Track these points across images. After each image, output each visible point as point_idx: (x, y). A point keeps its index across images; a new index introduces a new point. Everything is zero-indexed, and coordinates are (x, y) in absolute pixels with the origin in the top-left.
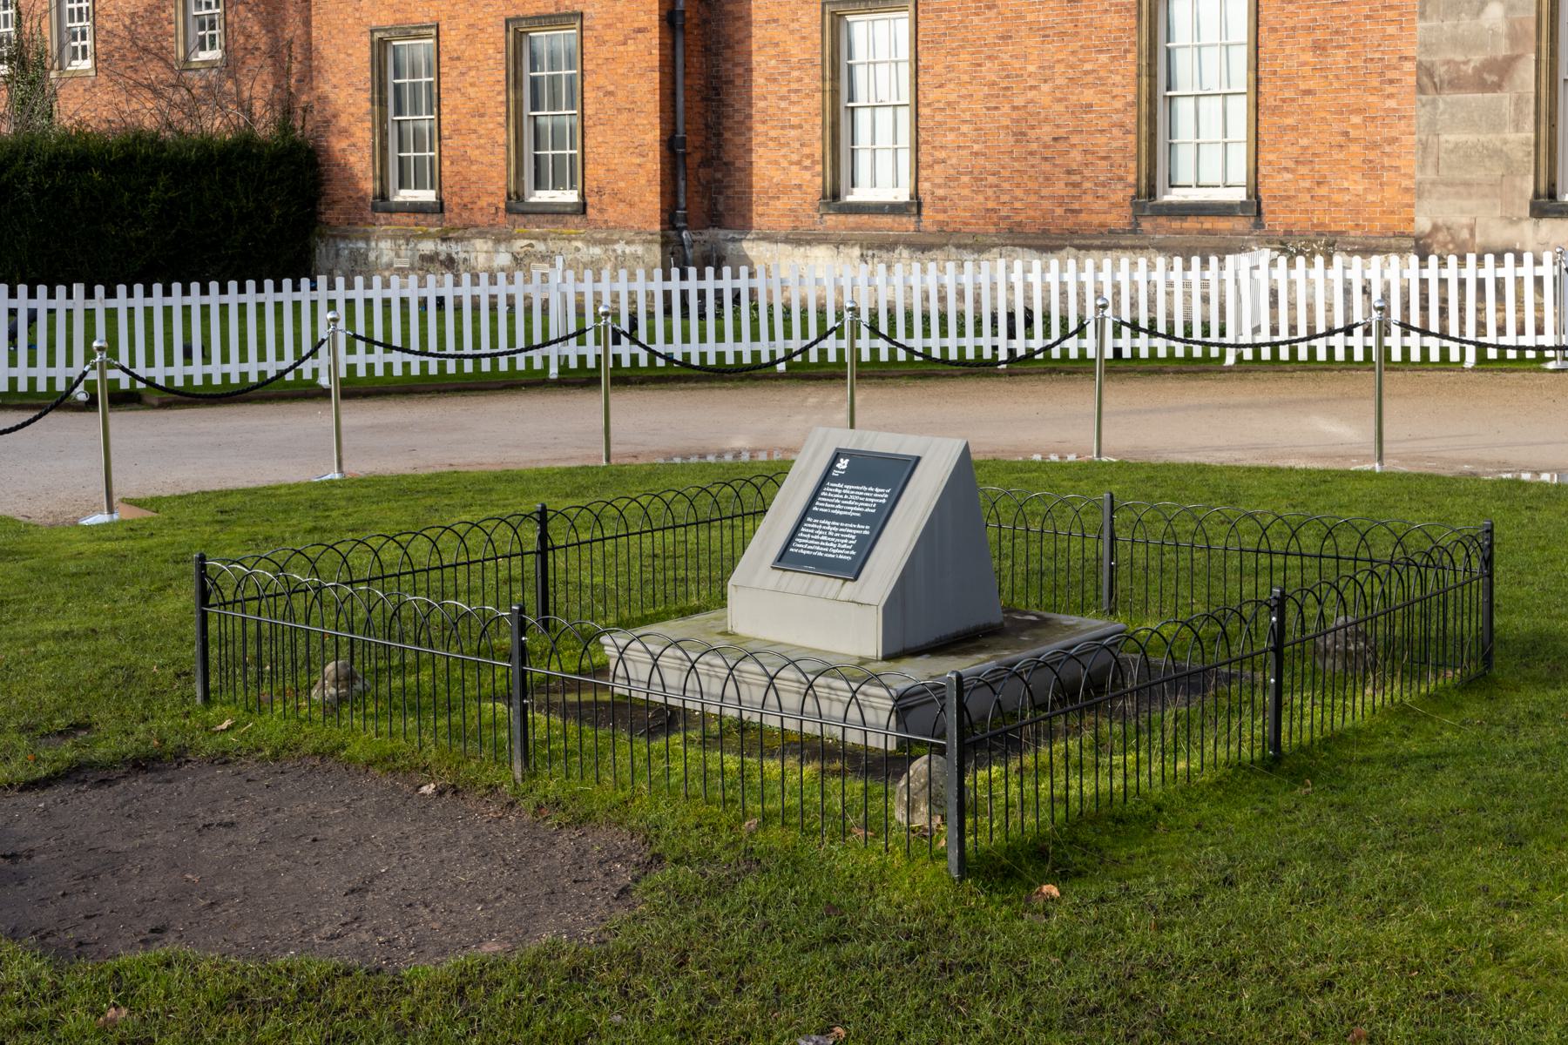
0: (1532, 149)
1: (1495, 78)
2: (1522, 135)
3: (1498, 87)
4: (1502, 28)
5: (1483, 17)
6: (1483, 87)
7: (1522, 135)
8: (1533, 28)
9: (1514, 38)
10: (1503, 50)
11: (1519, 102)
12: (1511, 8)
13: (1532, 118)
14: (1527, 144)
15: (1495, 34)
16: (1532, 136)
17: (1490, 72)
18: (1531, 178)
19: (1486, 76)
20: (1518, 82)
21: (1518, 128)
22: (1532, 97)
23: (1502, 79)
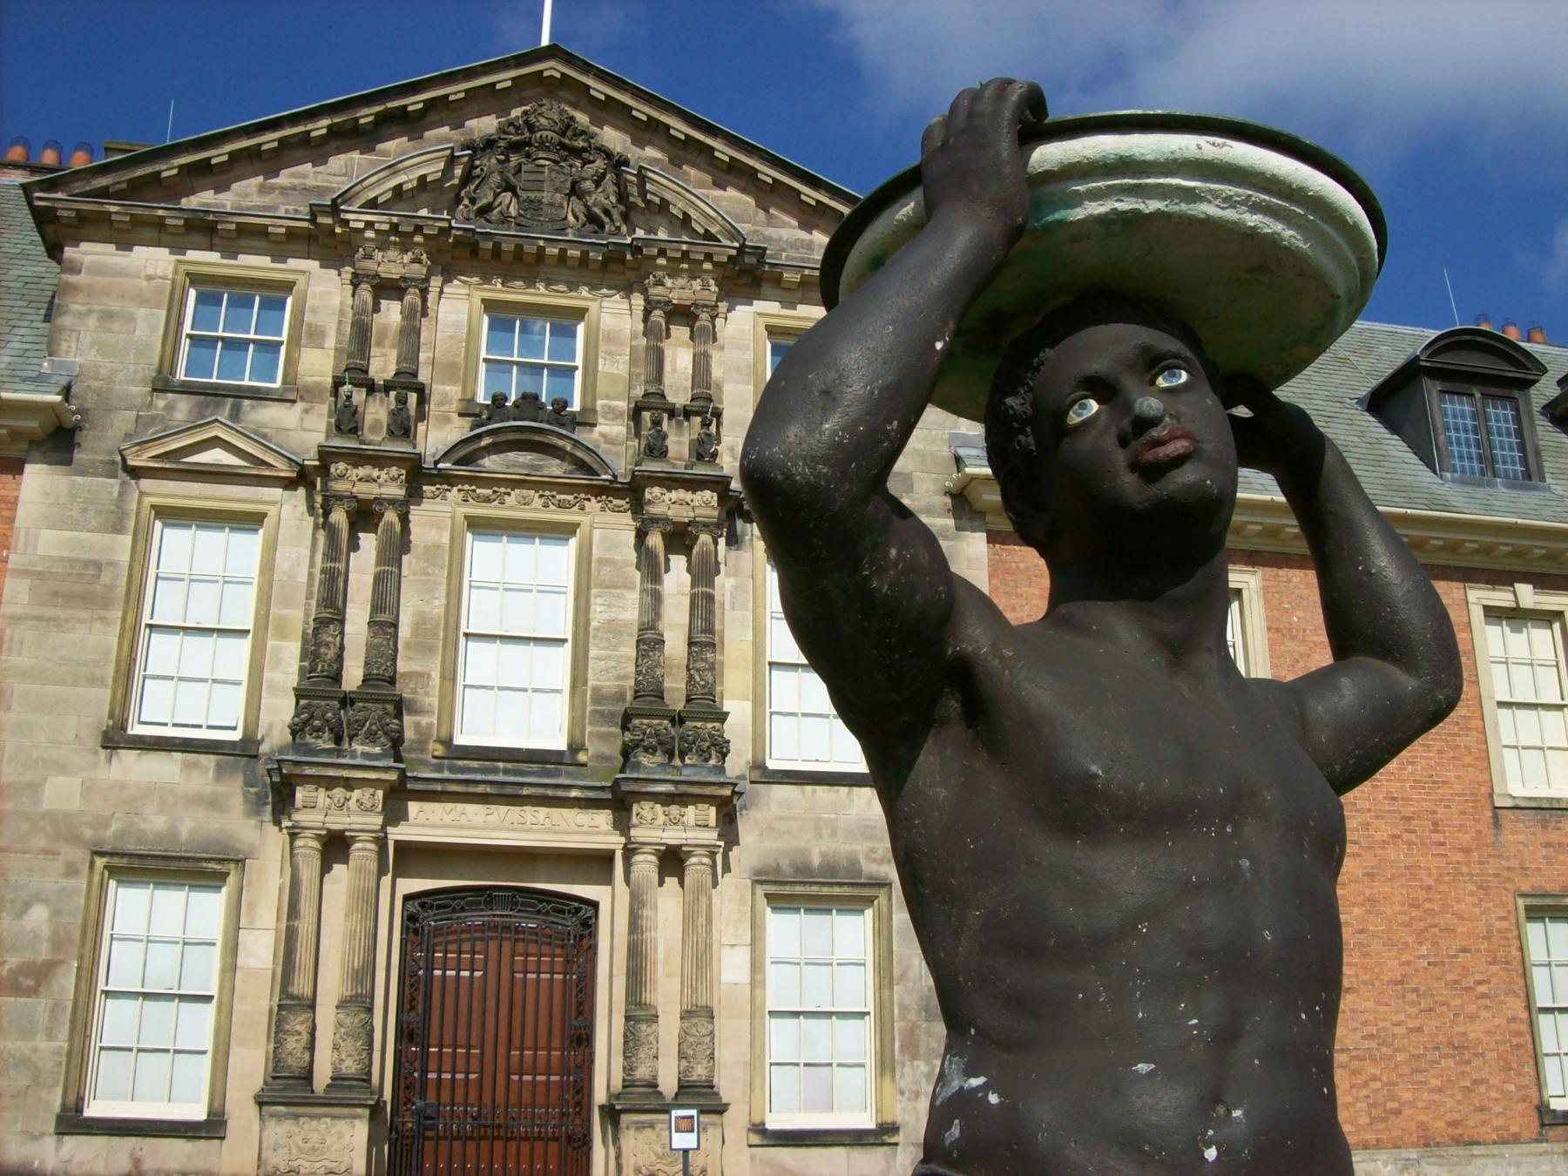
0: (64, 1059)
1: (30, 982)
2: (56, 1044)
3: (33, 991)
4: (46, 931)
5: (26, 918)
6: (18, 991)
7: (56, 1044)
8: (77, 934)
9: (57, 943)
10: (44, 953)
11: (55, 1010)
12: (56, 912)
13: (67, 1027)
14: (59, 1054)
15: (36, 936)
16: (66, 1045)
17: (26, 976)
18: (59, 1091)
19: (21, 979)
20: (56, 988)
21: (50, 1036)
22: (70, 1003)
23: (38, 984)
